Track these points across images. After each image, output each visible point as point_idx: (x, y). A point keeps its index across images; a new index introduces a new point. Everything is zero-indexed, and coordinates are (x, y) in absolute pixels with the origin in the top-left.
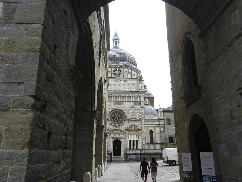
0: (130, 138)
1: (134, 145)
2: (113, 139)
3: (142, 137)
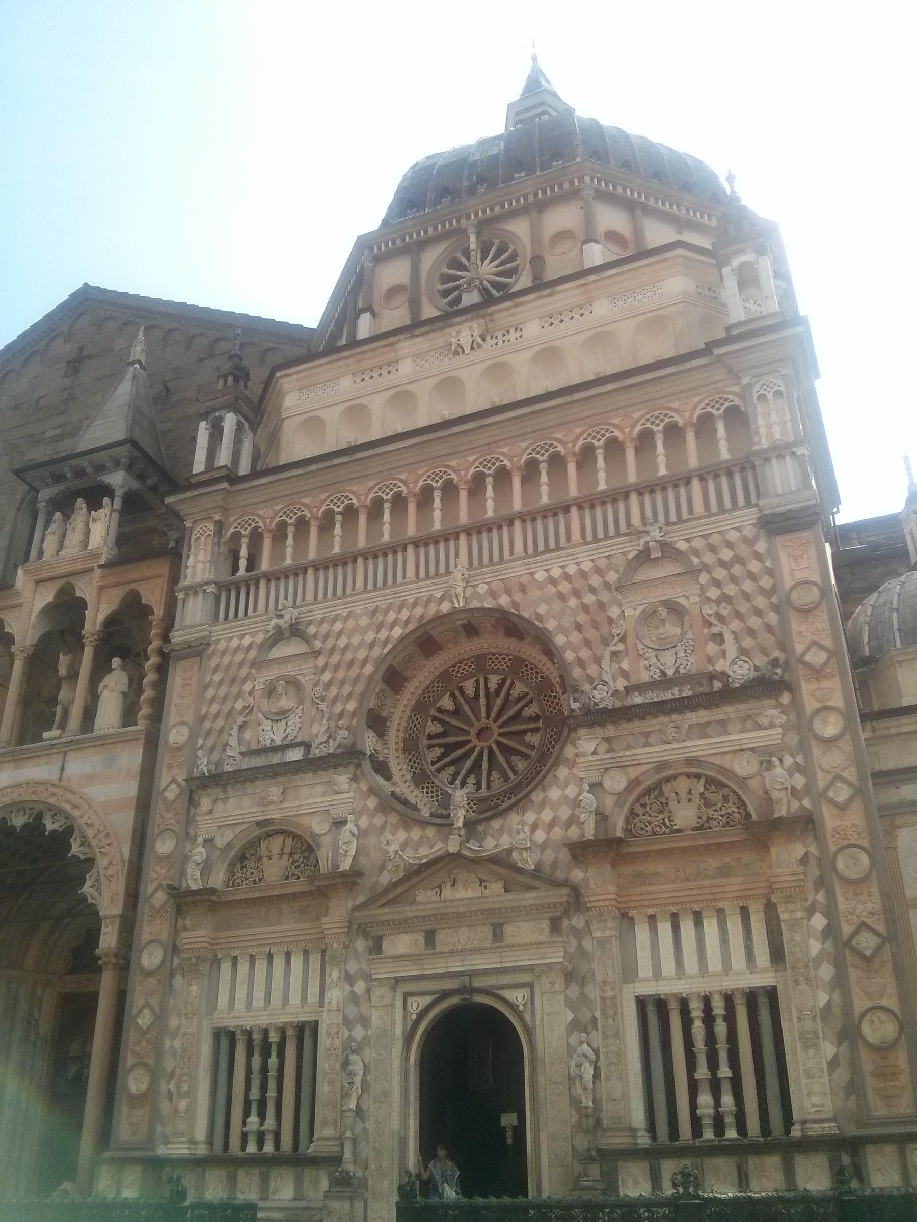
0: (644, 968)
1: (725, 1072)
2: (417, 1004)
3: (830, 931)
